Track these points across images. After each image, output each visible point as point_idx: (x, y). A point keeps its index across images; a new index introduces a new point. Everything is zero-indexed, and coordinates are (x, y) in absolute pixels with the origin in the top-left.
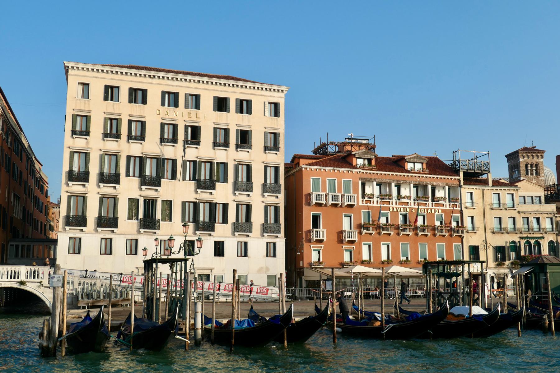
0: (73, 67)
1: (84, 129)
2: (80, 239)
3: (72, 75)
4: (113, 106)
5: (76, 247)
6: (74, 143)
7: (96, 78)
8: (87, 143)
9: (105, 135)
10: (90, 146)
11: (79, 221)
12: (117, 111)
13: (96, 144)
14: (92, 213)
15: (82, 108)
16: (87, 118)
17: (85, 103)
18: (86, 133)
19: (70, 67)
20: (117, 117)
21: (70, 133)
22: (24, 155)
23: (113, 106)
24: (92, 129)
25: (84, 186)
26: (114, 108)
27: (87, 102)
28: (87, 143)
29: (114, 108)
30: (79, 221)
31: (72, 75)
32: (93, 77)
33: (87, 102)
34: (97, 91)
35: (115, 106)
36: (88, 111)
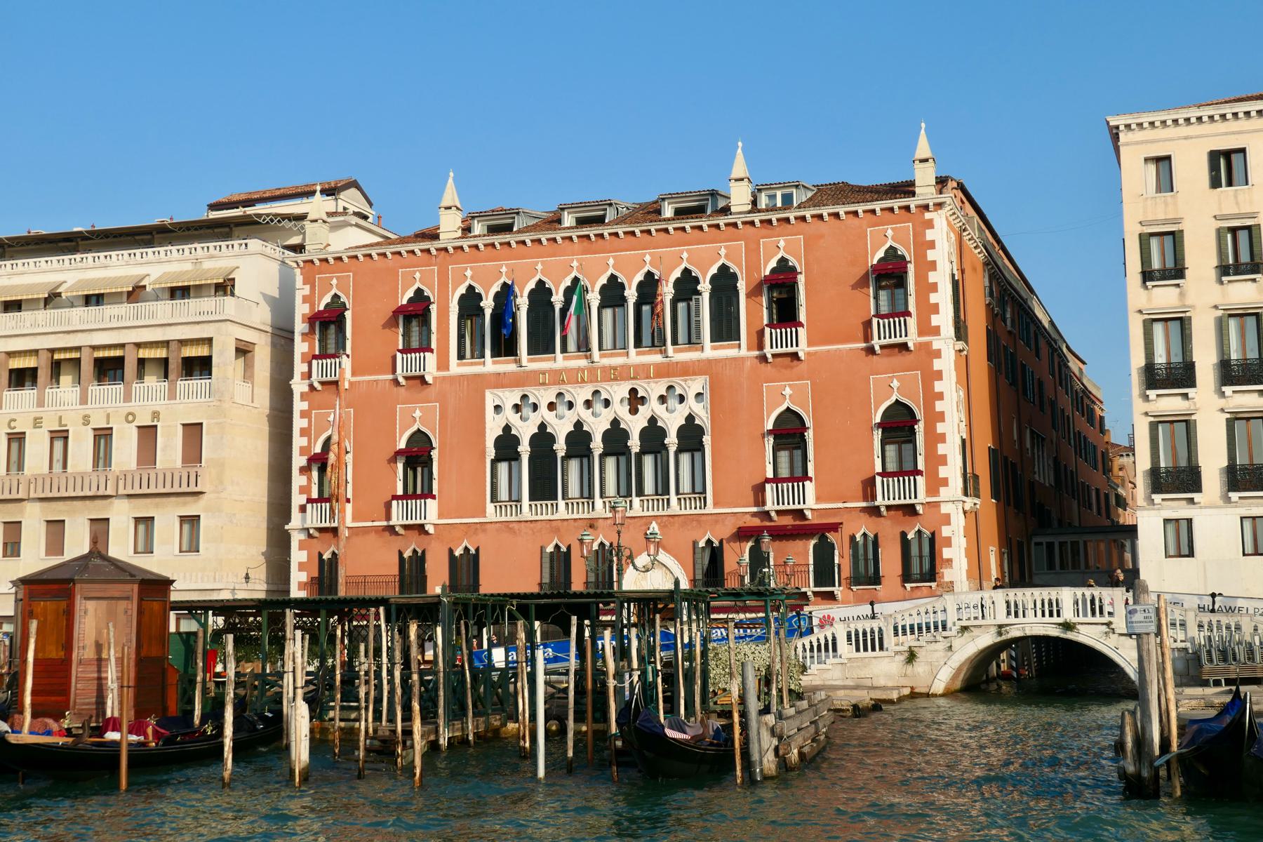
0: (1128, 126)
1: (1170, 264)
2: (1190, 521)
3: (1127, 144)
4: (1236, 197)
5: (1182, 542)
6: (1149, 299)
7: (1186, 138)
8: (1182, 295)
9: (1224, 270)
10: (1189, 302)
11: (1180, 479)
12: (1246, 209)
13: (1204, 294)
14: (1212, 458)
15: (1161, 216)
16: (1176, 237)
17: (1166, 204)
18: (1177, 272)
19: (1122, 128)
20: (1249, 222)
21: (1139, 278)
22: (1042, 343)
23: (1236, 197)
24: (1189, 261)
25: (1185, 396)
26: (1237, 203)
27: (1169, 199)
28: (1182, 295)
29: (1237, 203)
30: (1180, 479)
31: (1127, 144)
32: (1179, 138)
33: (1169, 199)
34: (1191, 168)
35: (1241, 198)
36: (1176, 221)
